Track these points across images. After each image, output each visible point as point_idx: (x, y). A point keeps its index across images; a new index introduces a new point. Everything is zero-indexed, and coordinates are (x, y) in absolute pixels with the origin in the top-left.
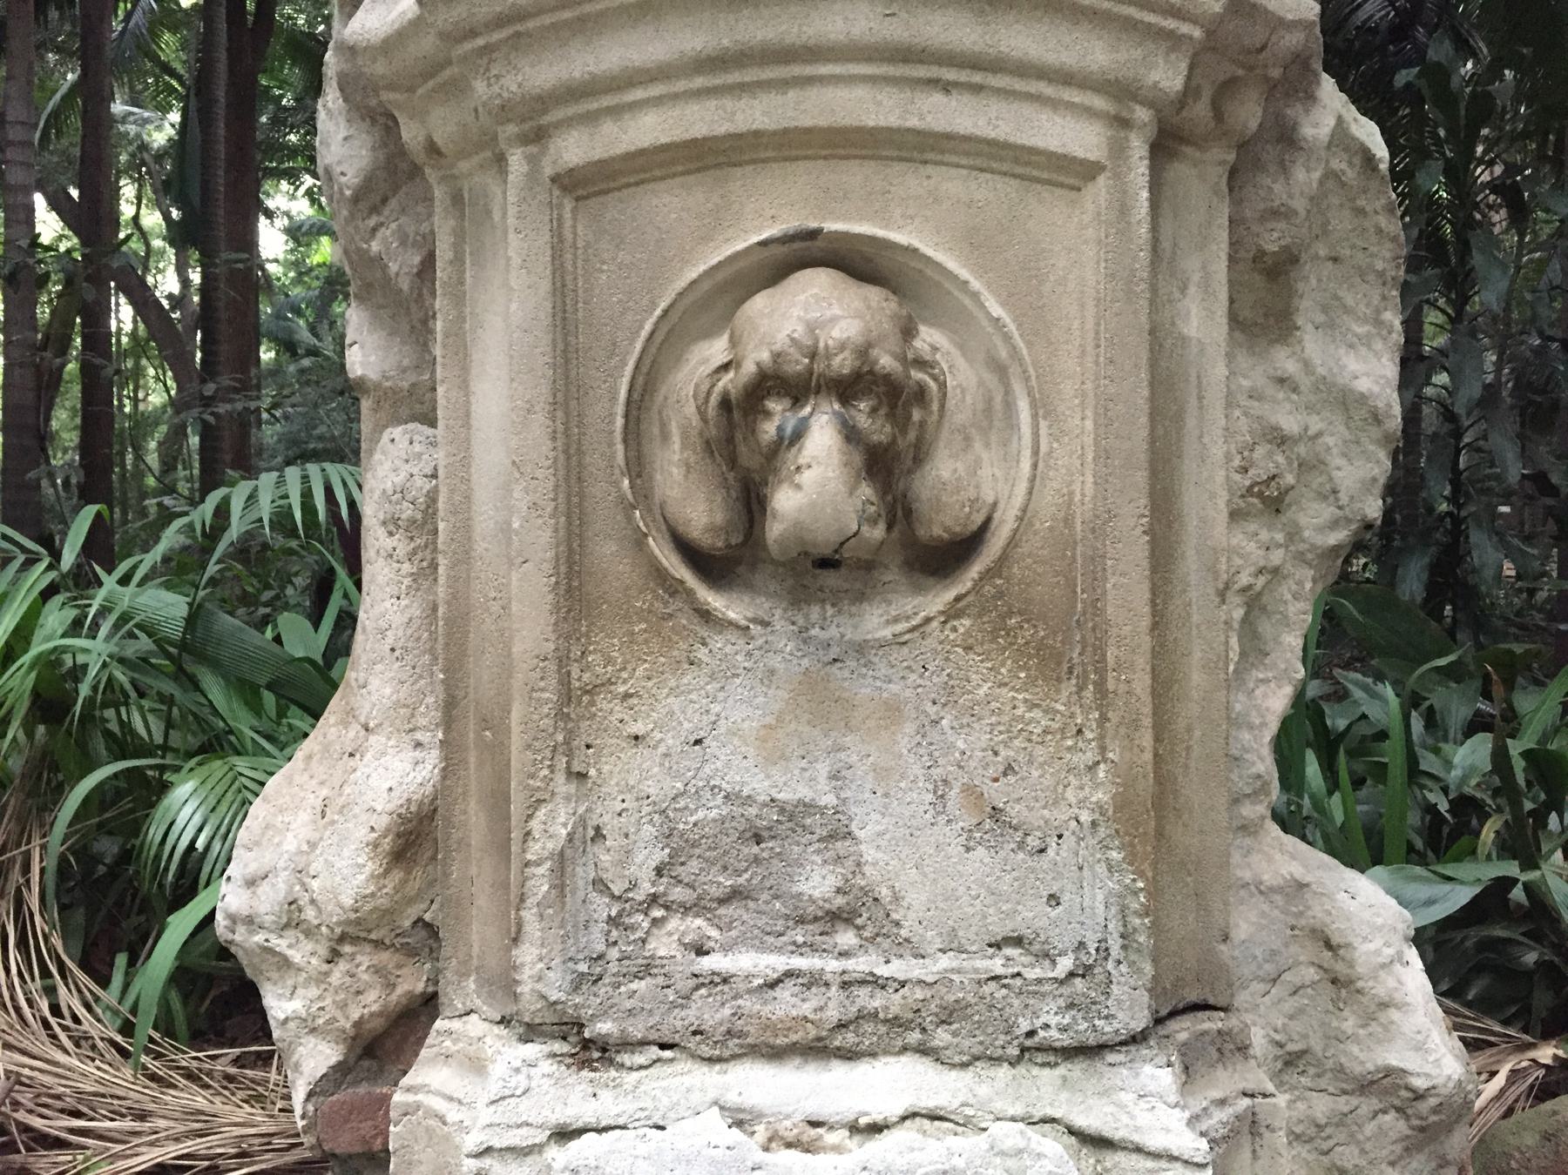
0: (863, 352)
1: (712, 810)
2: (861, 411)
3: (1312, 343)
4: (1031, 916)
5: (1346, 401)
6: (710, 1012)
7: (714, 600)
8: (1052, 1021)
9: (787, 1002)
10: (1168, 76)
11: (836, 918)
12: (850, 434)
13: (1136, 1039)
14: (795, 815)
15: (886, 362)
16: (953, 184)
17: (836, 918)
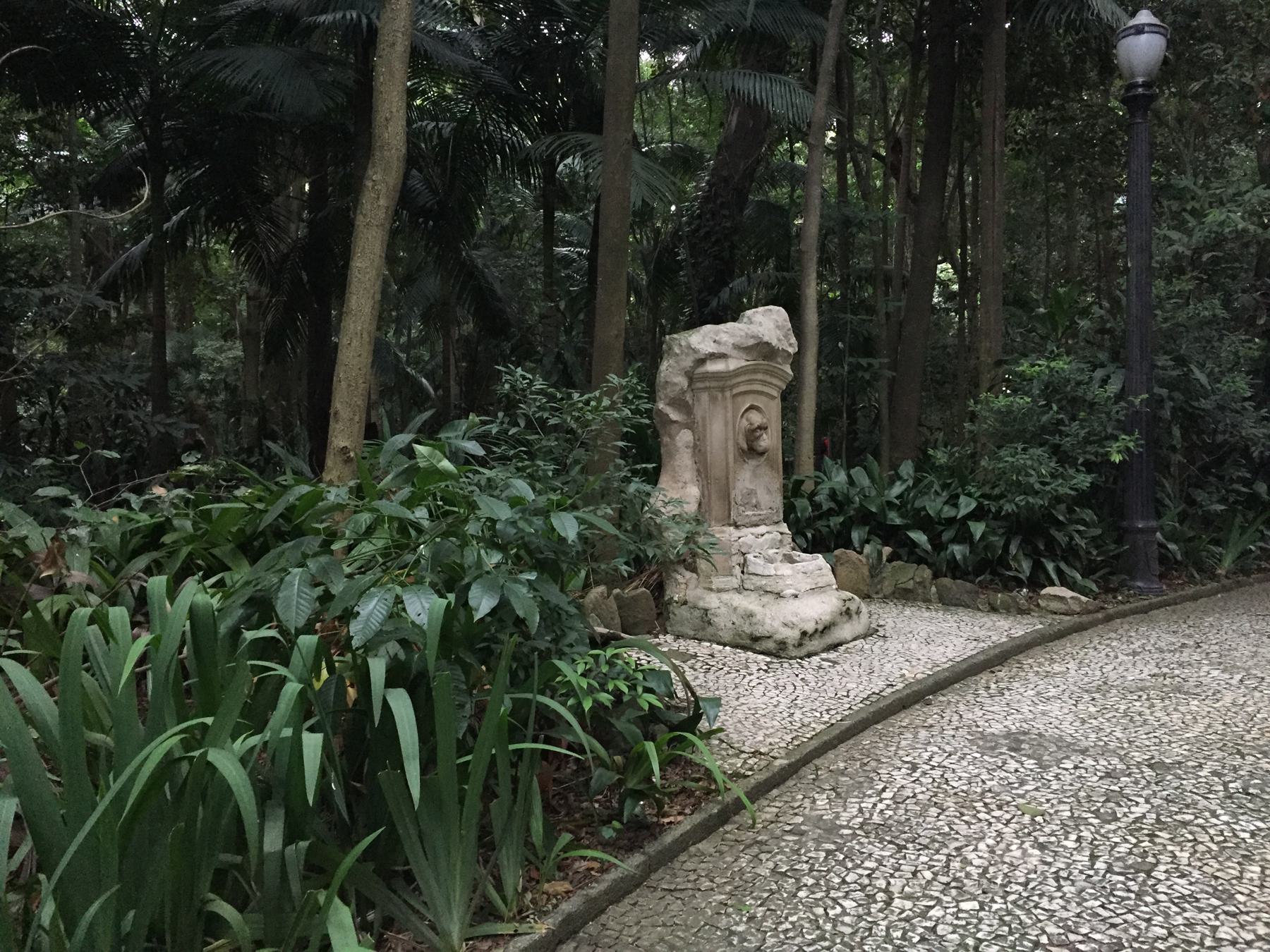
4: (772, 505)
6: (747, 520)
8: (776, 519)
9: (754, 519)
16: (764, 398)
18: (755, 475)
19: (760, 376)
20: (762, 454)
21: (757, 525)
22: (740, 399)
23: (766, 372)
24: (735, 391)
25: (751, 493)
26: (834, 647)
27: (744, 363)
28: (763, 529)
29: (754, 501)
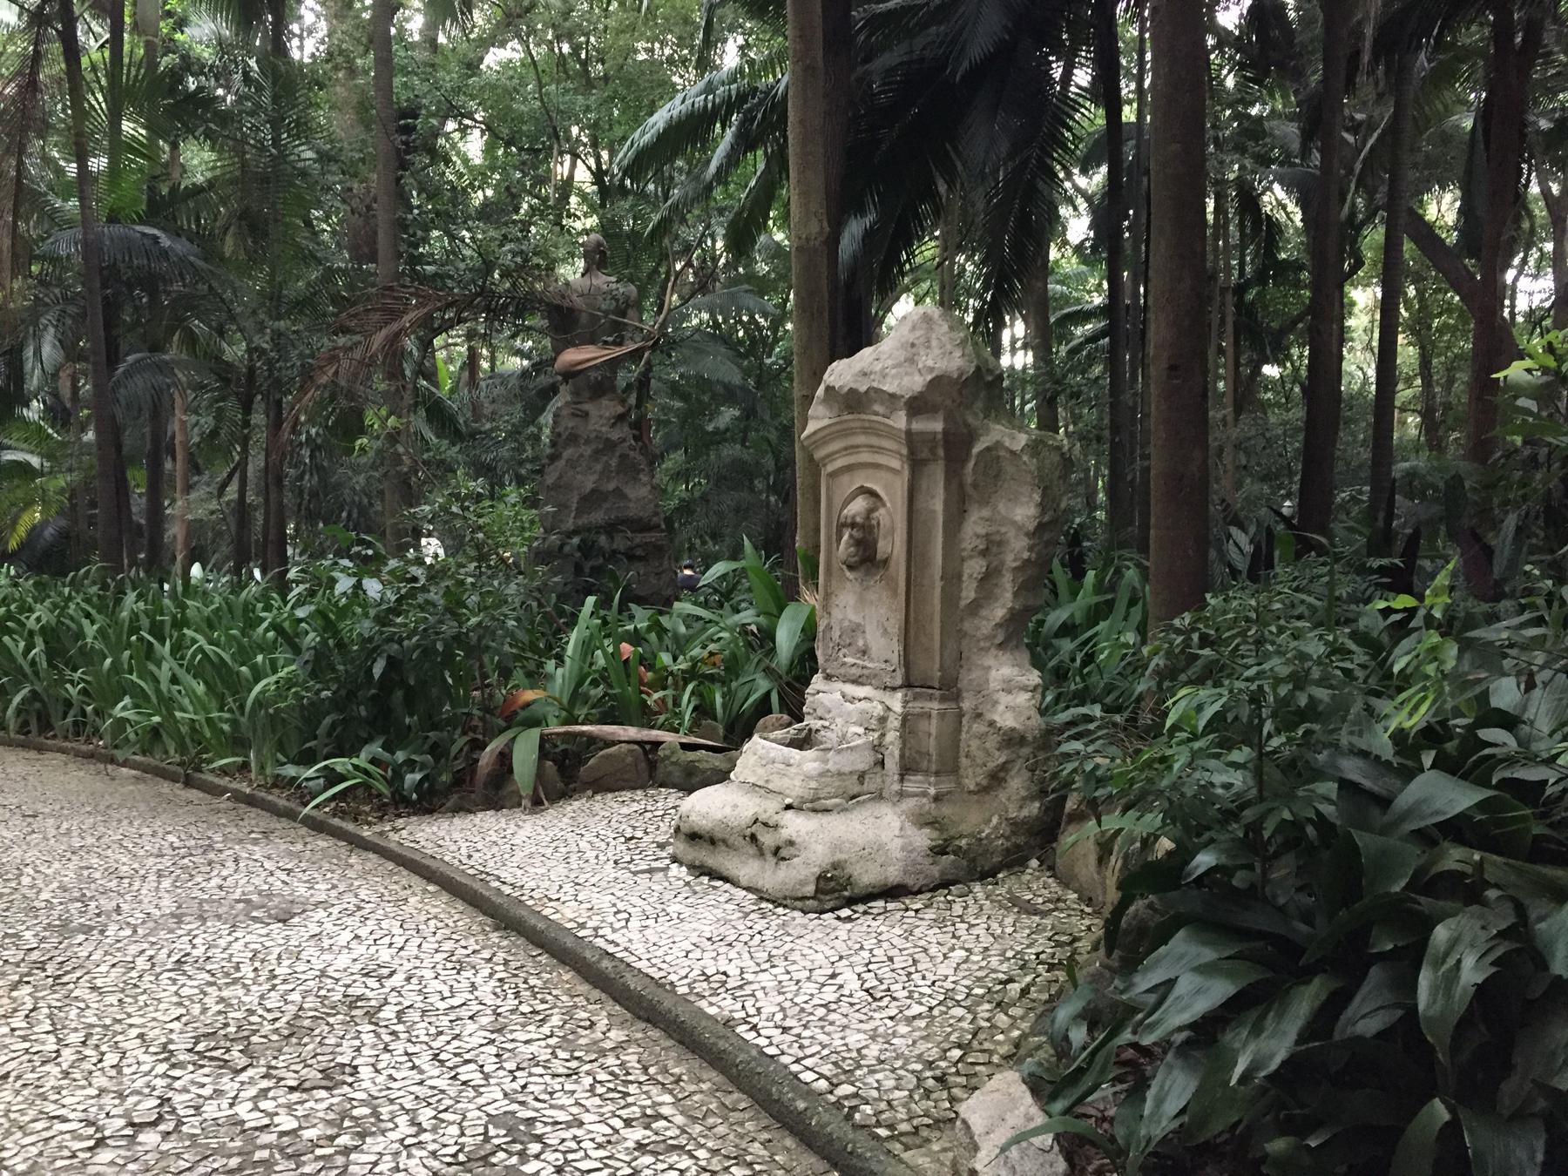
0: (854, 517)
1: (846, 624)
2: (854, 532)
3: (1002, 507)
4: (888, 656)
5: (1014, 523)
6: (842, 671)
7: (848, 574)
8: (888, 681)
9: (854, 670)
10: (905, 451)
11: (864, 653)
12: (851, 536)
13: (900, 687)
14: (859, 625)
15: (858, 520)
16: (882, 474)
17: (864, 653)
18: (861, 601)
19: (861, 439)
20: (886, 562)
21: (856, 681)
22: (845, 478)
23: (866, 430)
24: (830, 468)
25: (857, 629)
26: (714, 875)
27: (826, 422)
28: (861, 691)
29: (861, 643)
